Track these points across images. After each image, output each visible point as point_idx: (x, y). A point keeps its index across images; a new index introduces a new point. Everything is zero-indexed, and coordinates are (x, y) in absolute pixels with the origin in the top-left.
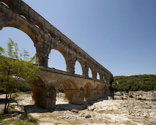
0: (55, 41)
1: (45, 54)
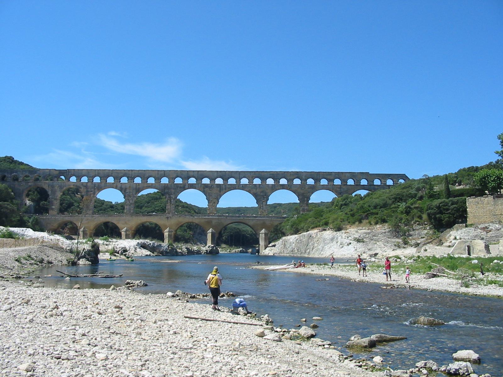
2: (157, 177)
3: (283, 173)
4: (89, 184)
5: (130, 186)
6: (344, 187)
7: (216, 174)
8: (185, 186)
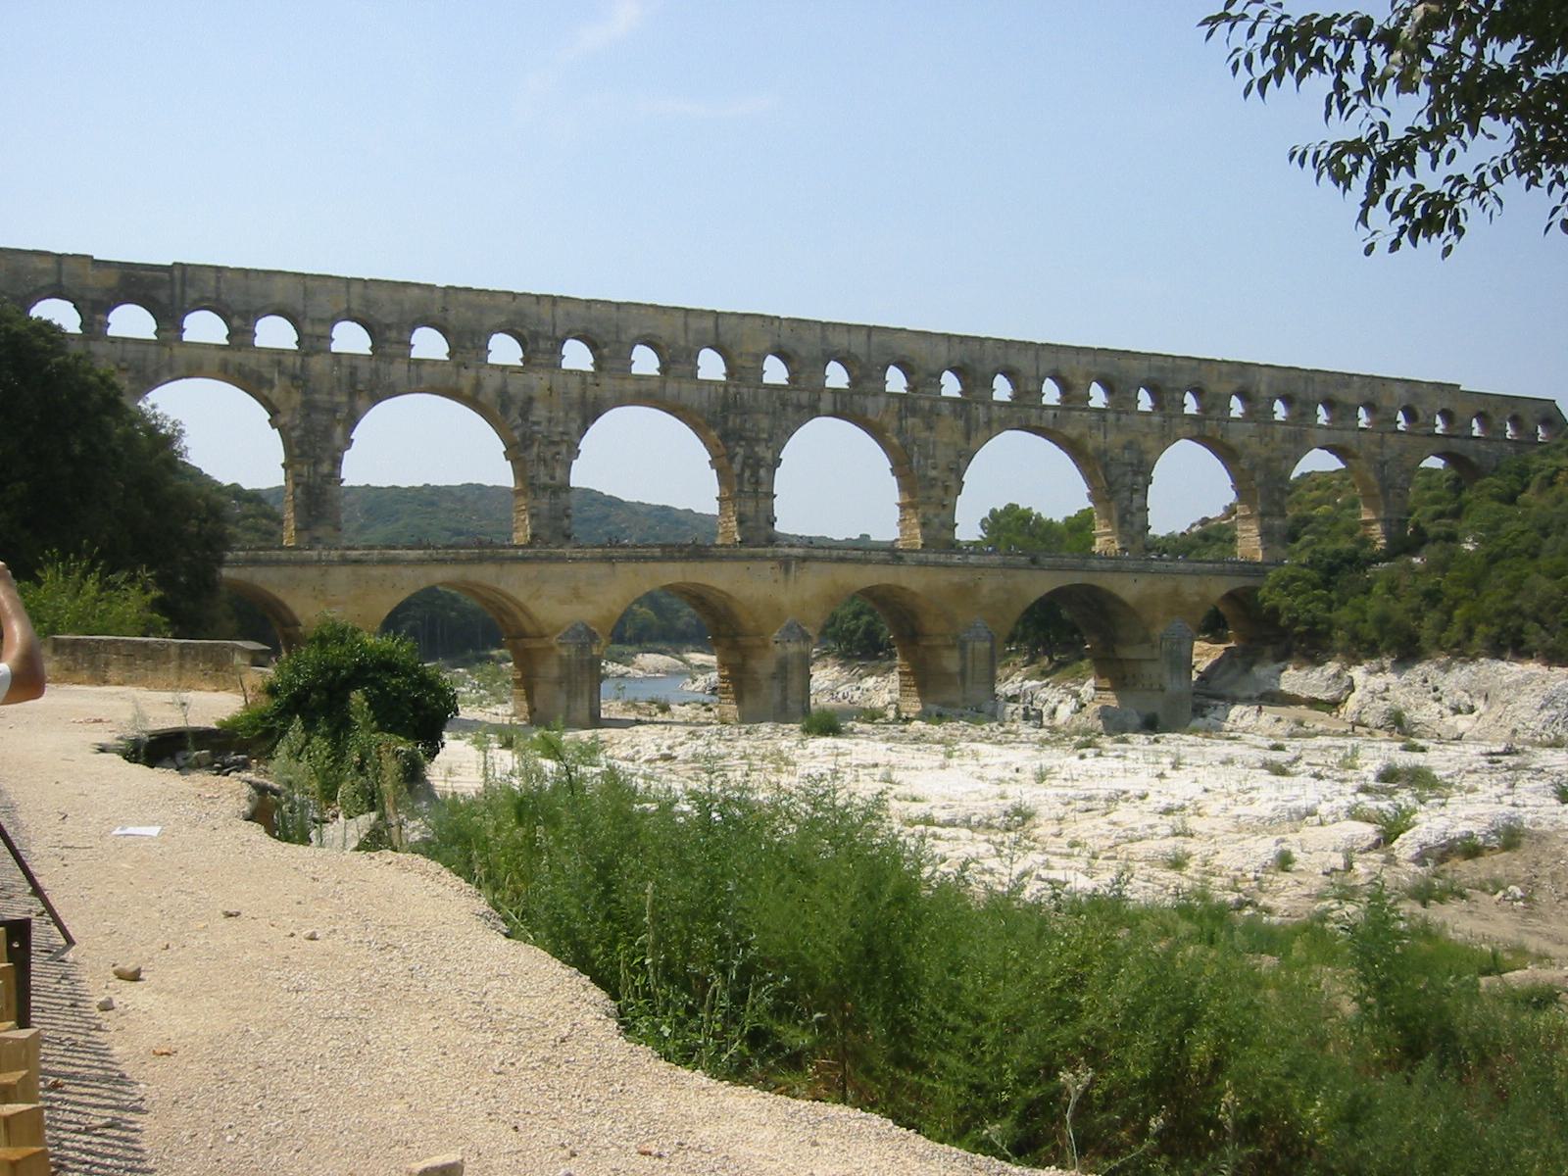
0: (382, 366)
1: (318, 462)
2: (682, 343)
4: (318, 364)
5: (550, 389)
6: (1391, 439)
8: (819, 399)
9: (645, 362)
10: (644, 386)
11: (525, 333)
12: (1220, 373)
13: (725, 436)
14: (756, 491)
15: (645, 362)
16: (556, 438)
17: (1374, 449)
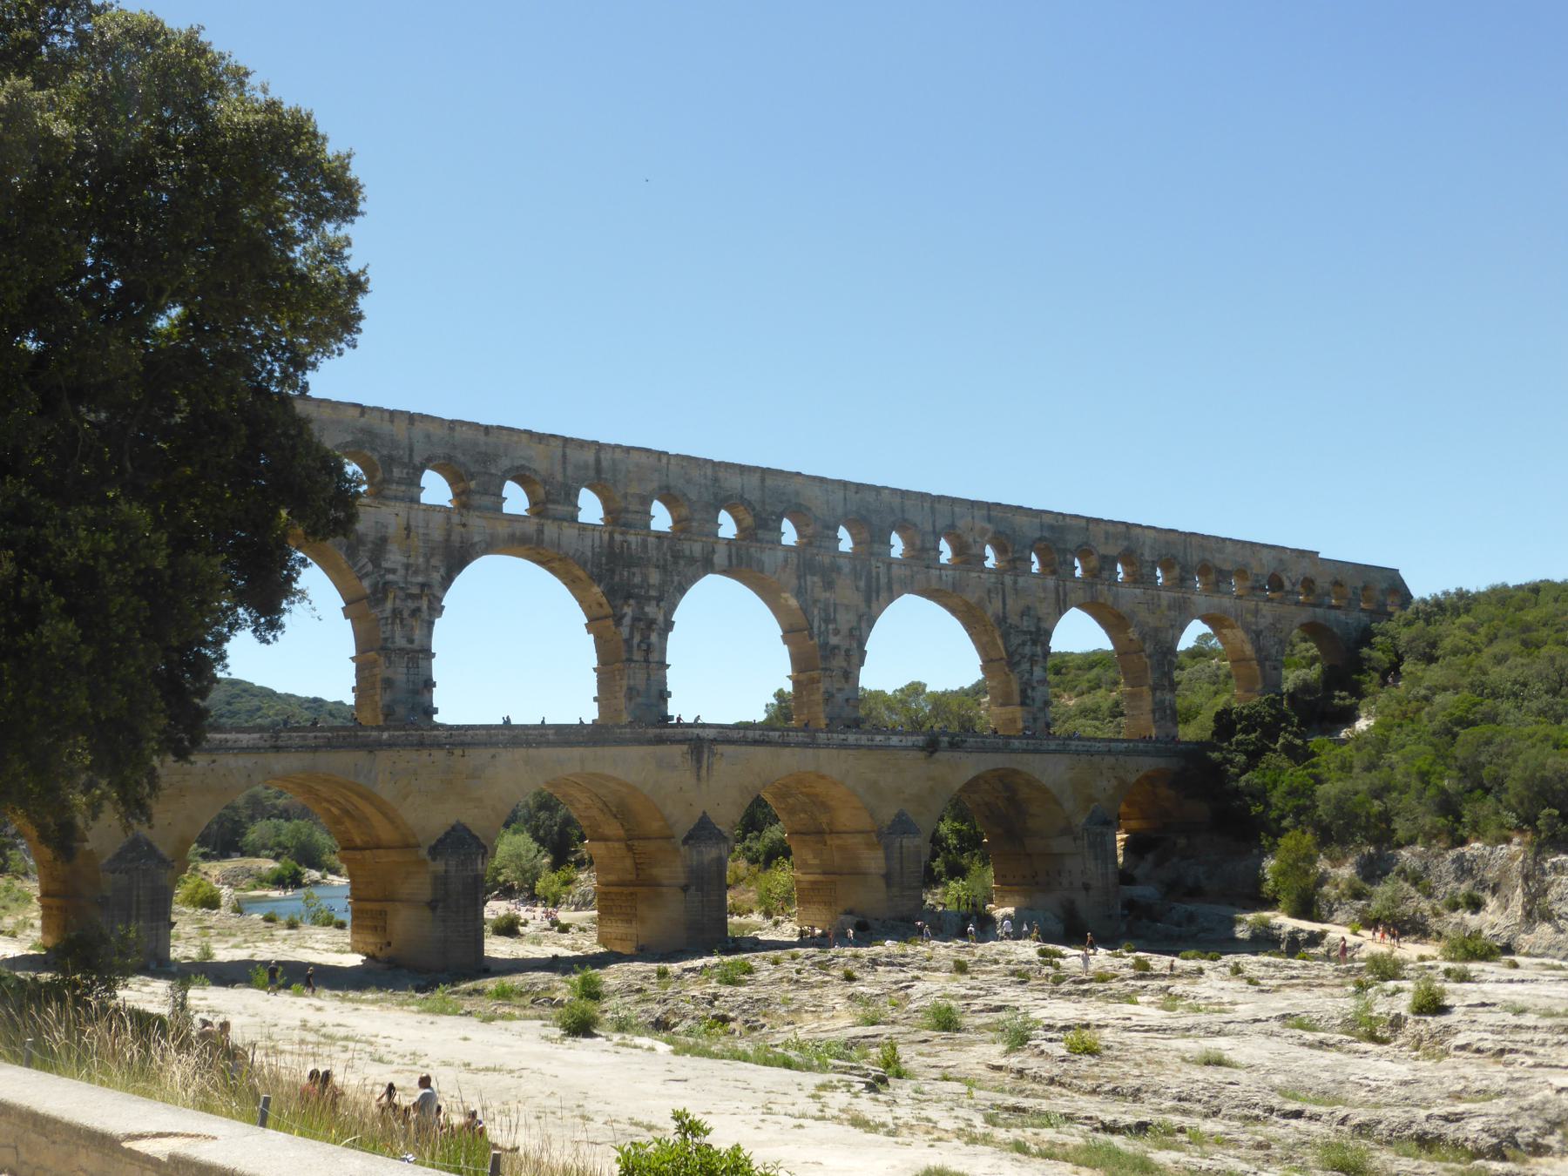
3: (1083, 523)
5: (408, 528)
7: (841, 494)
8: (713, 551)
9: (515, 500)
10: (518, 528)
11: (375, 458)
12: (1107, 533)
13: (610, 593)
14: (647, 661)
15: (515, 500)
16: (415, 590)
17: (1250, 618)
